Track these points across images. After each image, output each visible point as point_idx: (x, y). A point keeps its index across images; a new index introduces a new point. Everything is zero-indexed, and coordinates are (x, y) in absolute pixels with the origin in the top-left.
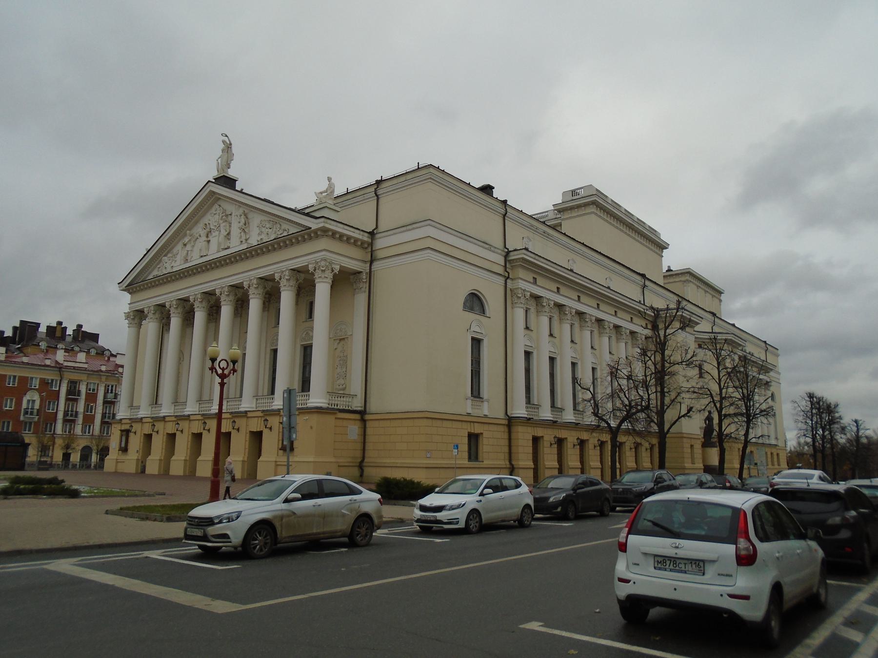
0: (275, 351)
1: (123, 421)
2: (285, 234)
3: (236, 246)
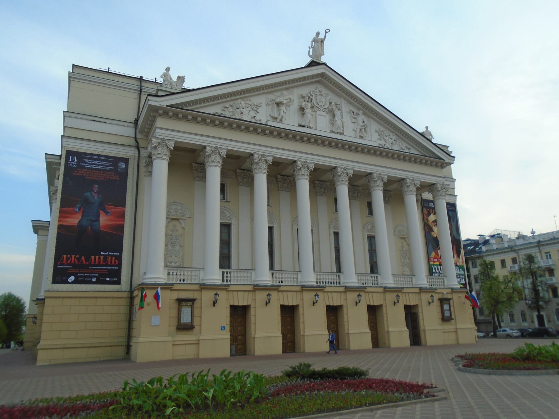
0: (336, 234)
2: (407, 151)
3: (349, 135)
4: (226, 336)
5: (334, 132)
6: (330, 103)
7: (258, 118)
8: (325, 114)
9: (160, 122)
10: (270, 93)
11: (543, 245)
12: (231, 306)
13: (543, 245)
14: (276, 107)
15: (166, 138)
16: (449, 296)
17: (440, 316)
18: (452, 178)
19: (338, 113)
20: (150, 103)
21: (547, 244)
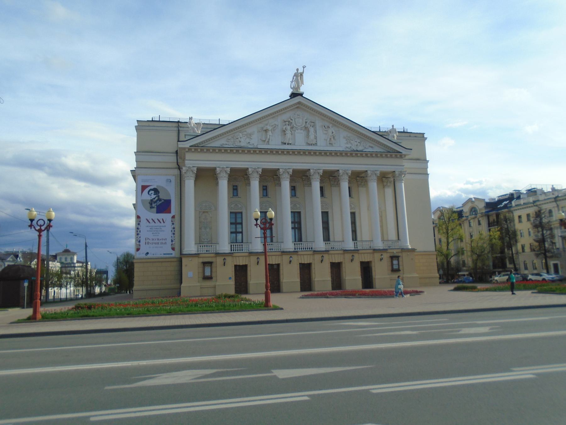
1: (201, 255)
2: (370, 150)
4: (232, 283)
5: (309, 144)
6: (306, 122)
7: (252, 142)
8: (302, 131)
9: (188, 156)
10: (260, 123)
11: (560, 200)
12: (236, 266)
13: (560, 200)
14: (264, 133)
15: (191, 166)
16: (400, 254)
17: (390, 268)
18: (426, 160)
19: (312, 130)
20: (180, 146)
21: (563, 200)
